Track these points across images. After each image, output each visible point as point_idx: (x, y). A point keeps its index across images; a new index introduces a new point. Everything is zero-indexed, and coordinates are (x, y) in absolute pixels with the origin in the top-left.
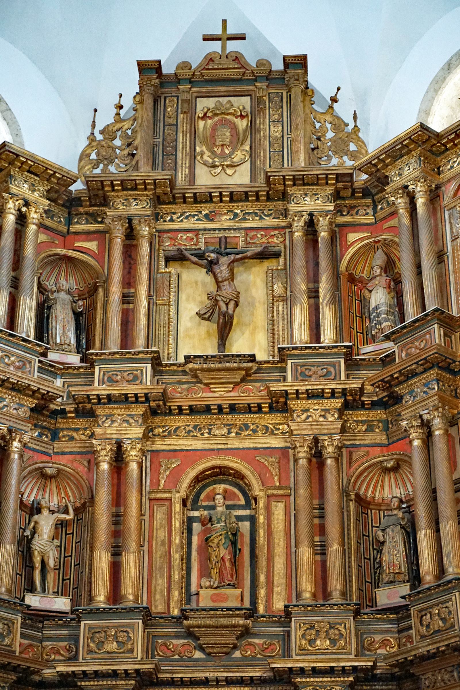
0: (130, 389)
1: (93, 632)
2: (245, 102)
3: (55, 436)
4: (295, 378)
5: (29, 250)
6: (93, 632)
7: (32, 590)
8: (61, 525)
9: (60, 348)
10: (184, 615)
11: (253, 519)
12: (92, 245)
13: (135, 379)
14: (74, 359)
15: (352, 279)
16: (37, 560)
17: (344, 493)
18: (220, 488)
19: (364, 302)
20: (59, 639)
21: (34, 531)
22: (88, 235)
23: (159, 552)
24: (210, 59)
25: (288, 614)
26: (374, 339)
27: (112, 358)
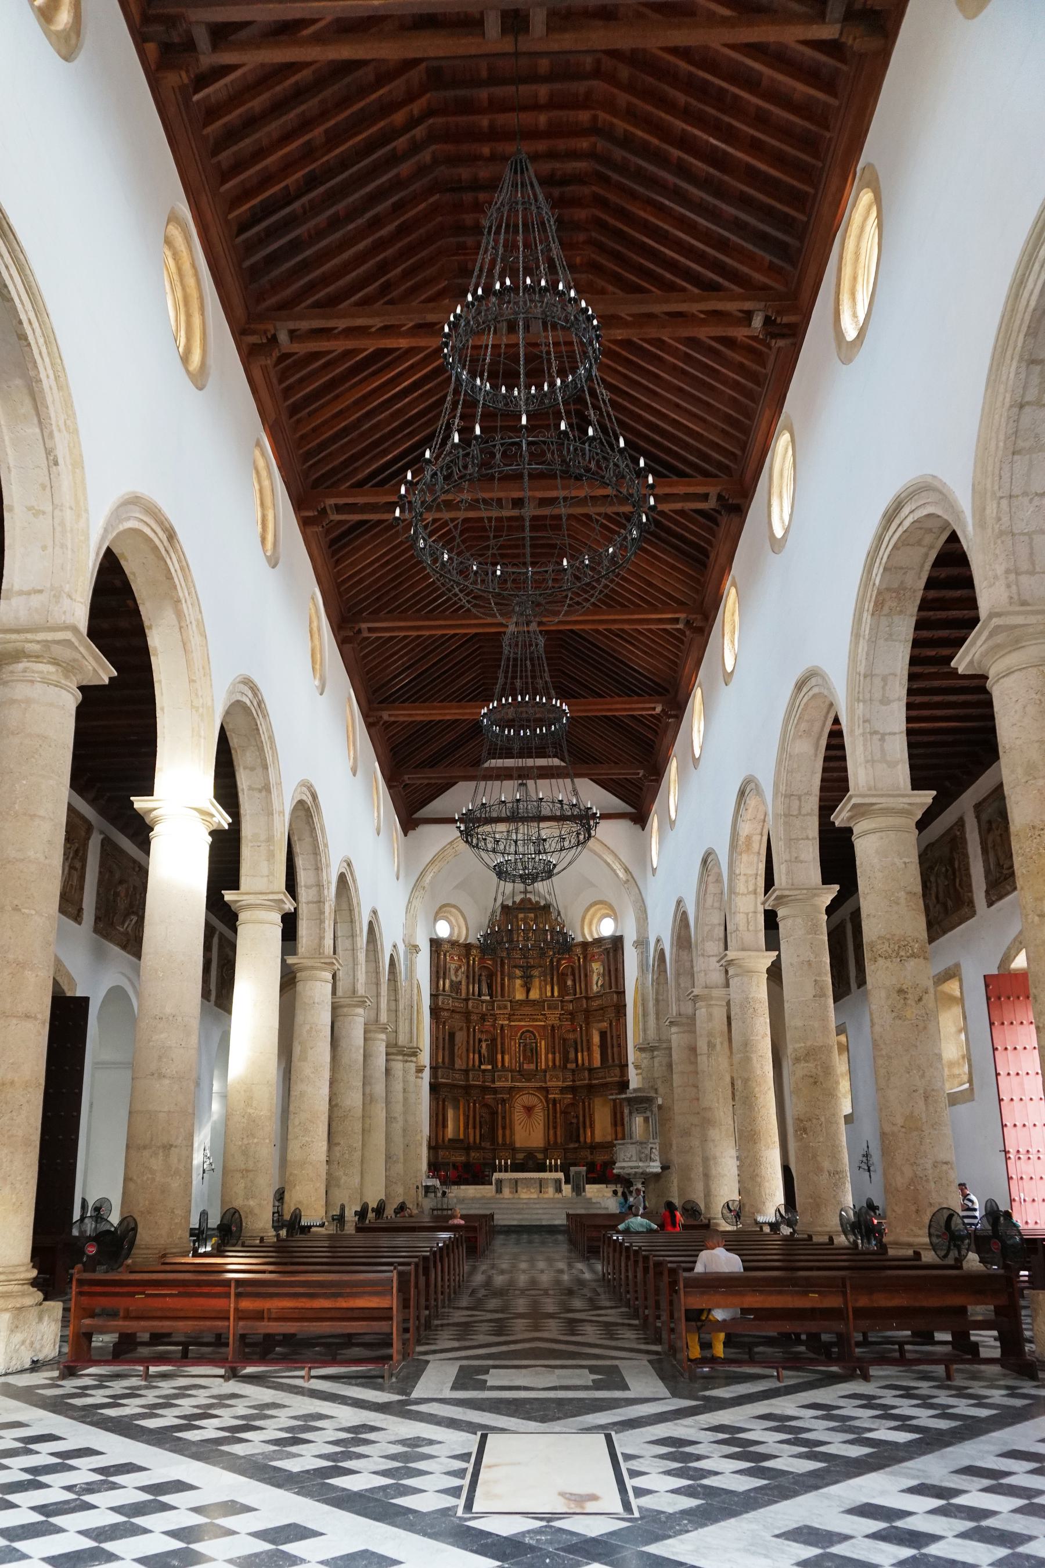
0: (505, 1012)
2: (532, 915)
4: (549, 1008)
10: (519, 1071)
11: (536, 1043)
13: (505, 1007)
14: (488, 998)
15: (563, 974)
17: (560, 1038)
18: (528, 1035)
19: (566, 983)
22: (489, 959)
23: (513, 1053)
24: (522, 901)
25: (545, 1071)
26: (568, 995)
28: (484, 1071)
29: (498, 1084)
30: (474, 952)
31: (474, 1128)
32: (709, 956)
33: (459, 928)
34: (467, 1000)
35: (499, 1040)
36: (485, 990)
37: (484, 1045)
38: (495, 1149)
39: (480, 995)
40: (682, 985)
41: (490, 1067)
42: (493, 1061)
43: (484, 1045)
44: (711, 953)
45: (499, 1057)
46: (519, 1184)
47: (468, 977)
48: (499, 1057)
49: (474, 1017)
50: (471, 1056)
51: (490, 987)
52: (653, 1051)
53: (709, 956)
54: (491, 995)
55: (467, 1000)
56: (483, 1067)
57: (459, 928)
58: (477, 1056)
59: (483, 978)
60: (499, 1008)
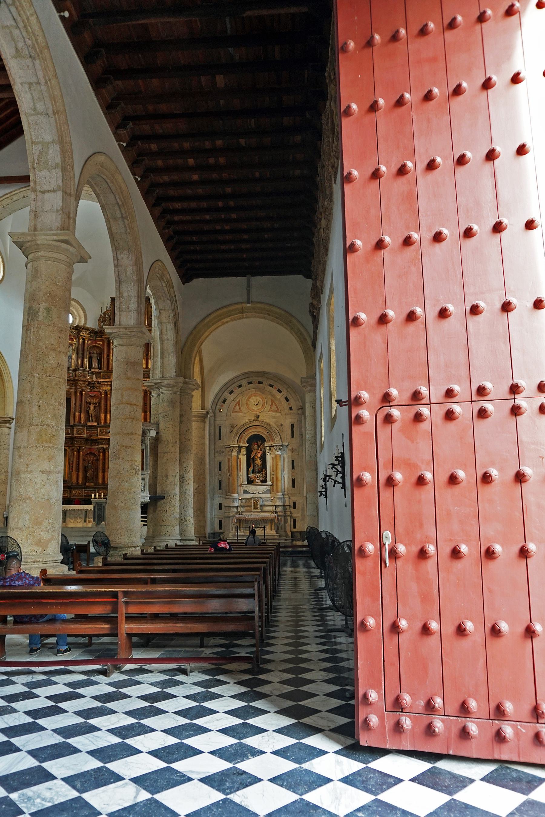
1: (101, 430)
3: (94, 388)
5: (86, 347)
6: (101, 430)
7: (89, 421)
8: (95, 406)
9: (94, 368)
12: (101, 343)
14: (97, 370)
16: (90, 415)
20: (95, 430)
21: (89, 409)
22: (100, 341)
27: (104, 372)
28: (91, 427)
29: (100, 437)
30: (83, 334)
31: (78, 471)
32: (43, 192)
33: (80, 318)
34: (75, 370)
35: (103, 402)
36: (95, 364)
37: (92, 407)
38: (95, 488)
39: (90, 367)
40: (125, 294)
41: (95, 424)
42: (98, 421)
43: (92, 407)
44: (47, 188)
45: (103, 416)
46: (68, 515)
47: (78, 353)
48: (103, 416)
49: (80, 385)
50: (77, 414)
51: (100, 362)
52: (158, 389)
53: (43, 192)
54: (100, 368)
55: (75, 370)
56: (89, 424)
57: (80, 318)
58: (83, 415)
59: (95, 355)
60: (104, 378)
